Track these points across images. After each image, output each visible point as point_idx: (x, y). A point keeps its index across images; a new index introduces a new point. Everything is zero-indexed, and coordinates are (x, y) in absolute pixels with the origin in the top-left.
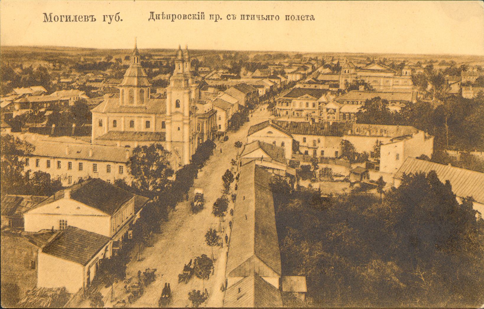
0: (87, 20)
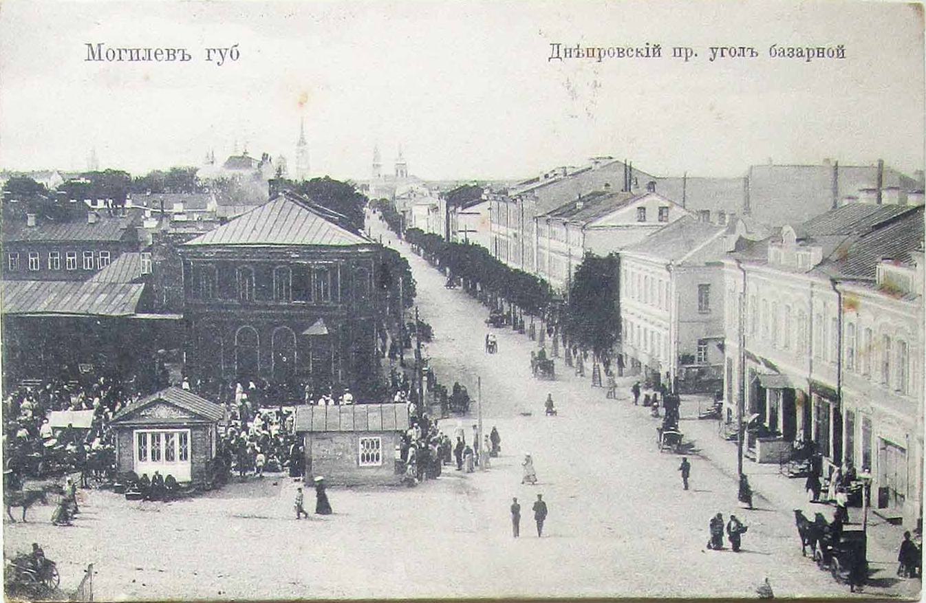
0: (172, 57)
